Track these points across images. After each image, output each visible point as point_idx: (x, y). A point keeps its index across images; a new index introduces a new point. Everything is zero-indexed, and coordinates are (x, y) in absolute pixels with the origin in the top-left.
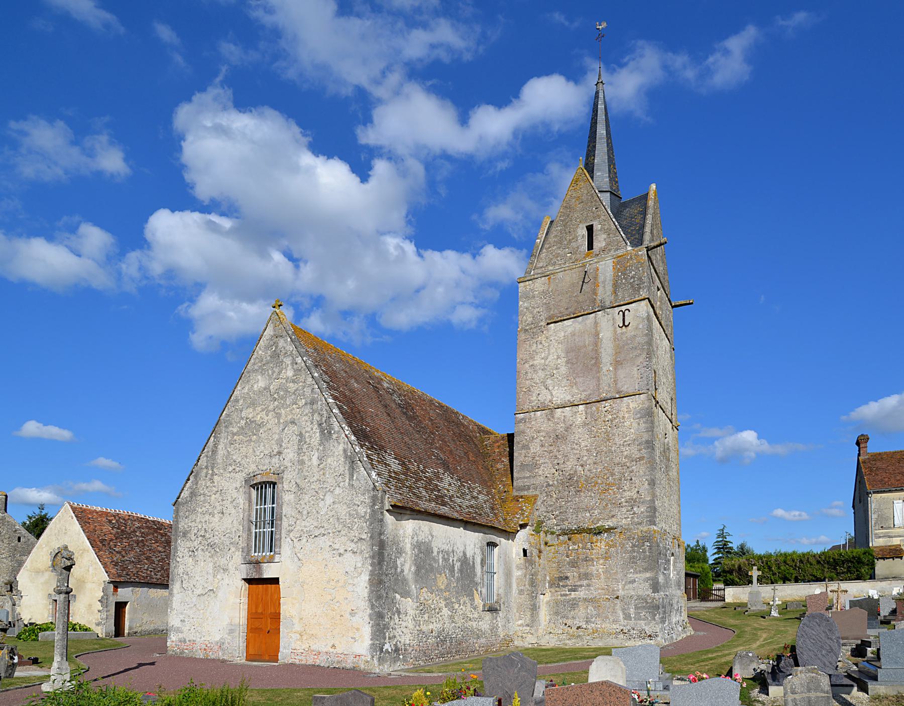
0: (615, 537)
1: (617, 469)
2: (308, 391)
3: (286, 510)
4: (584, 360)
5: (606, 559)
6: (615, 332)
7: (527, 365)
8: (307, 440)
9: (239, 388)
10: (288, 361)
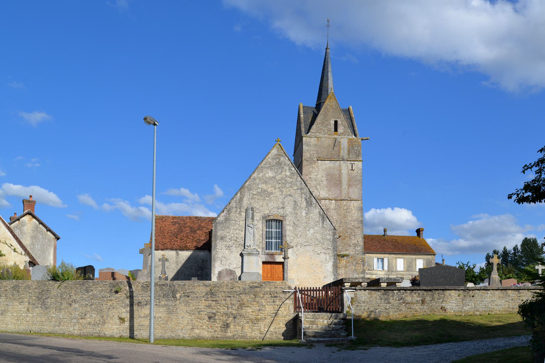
0: (349, 259)
1: (349, 231)
2: (299, 184)
3: (288, 233)
4: (334, 180)
5: (345, 268)
6: (348, 172)
7: (307, 177)
8: (299, 205)
9: (256, 173)
10: (287, 168)
